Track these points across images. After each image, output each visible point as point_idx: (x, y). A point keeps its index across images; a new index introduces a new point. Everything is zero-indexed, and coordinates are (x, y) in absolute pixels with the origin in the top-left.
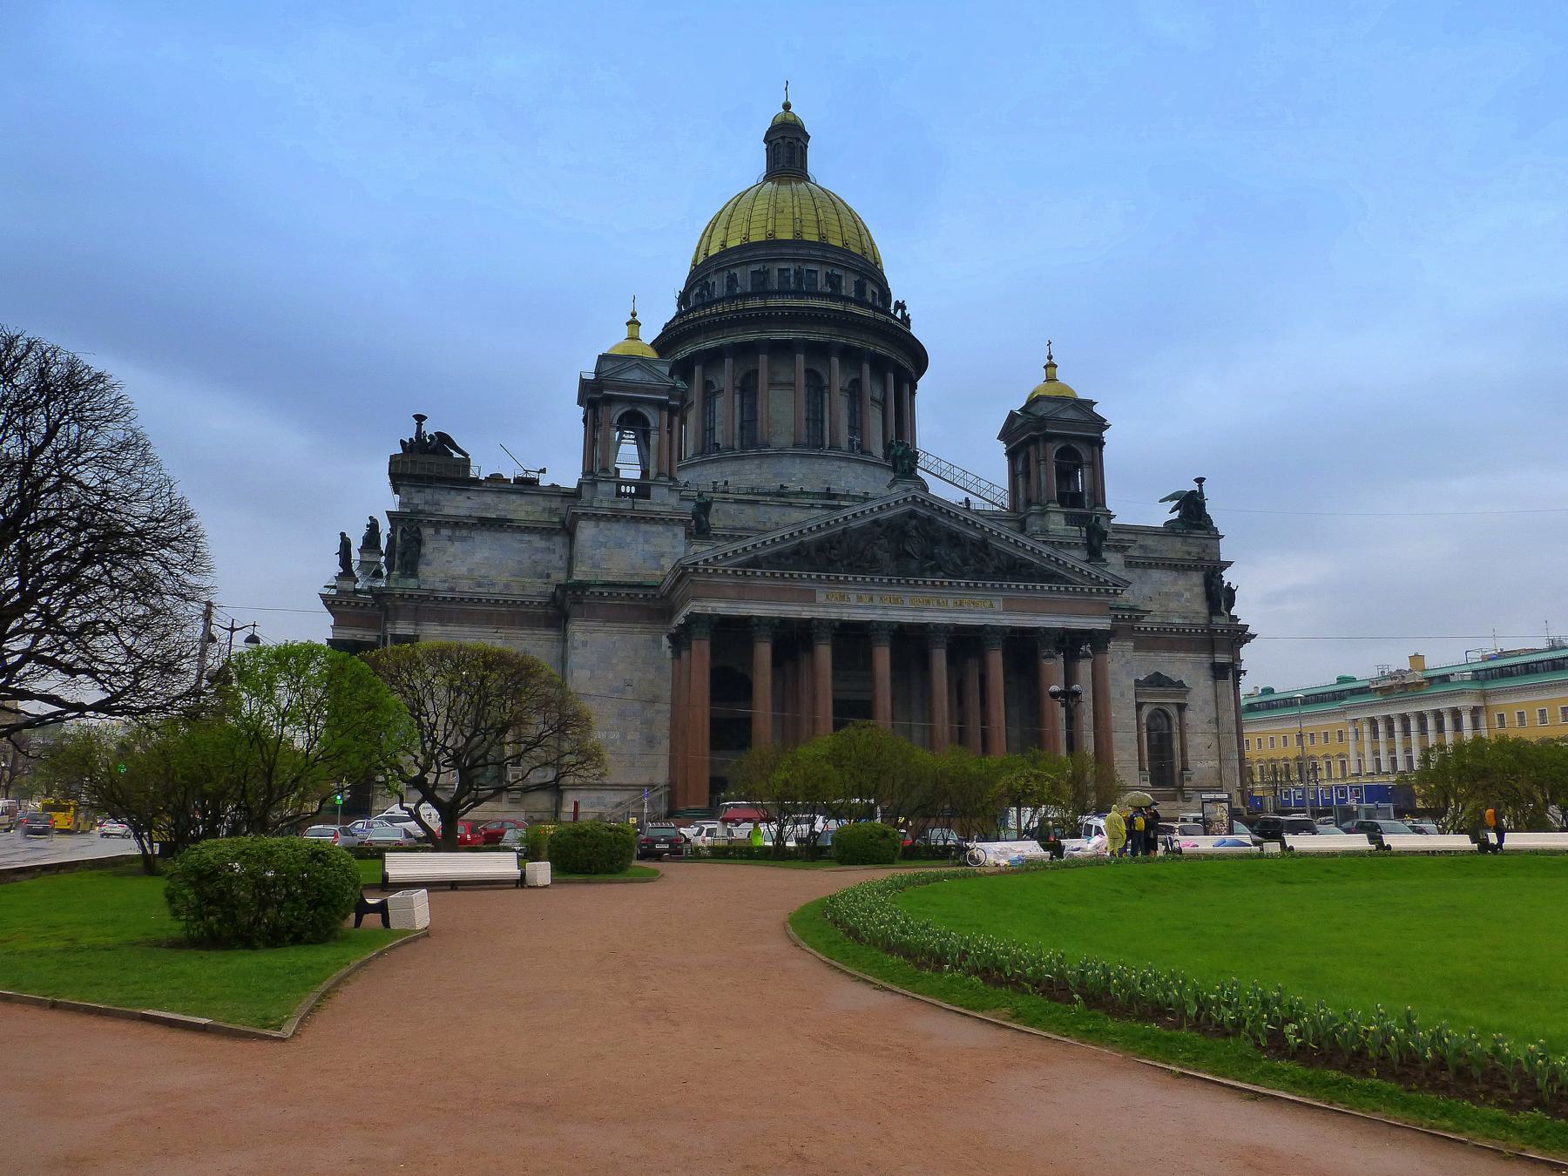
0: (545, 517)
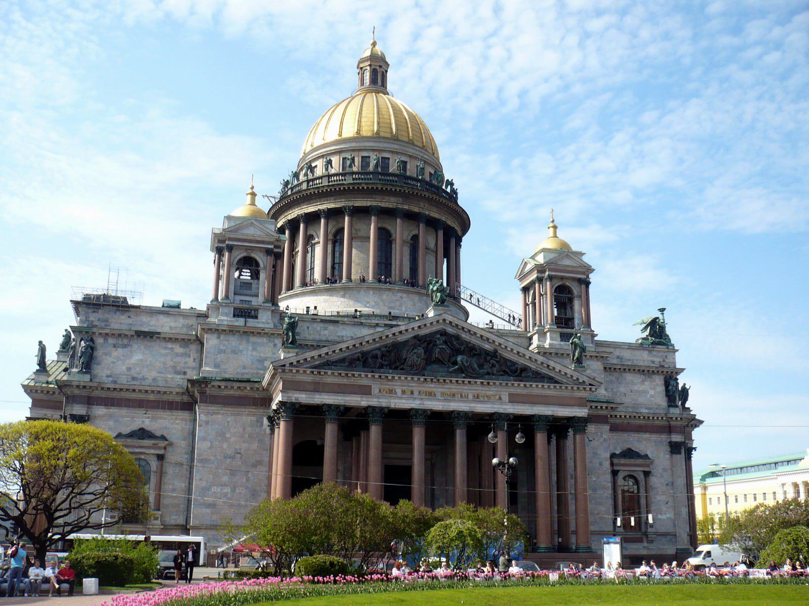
0: (184, 331)
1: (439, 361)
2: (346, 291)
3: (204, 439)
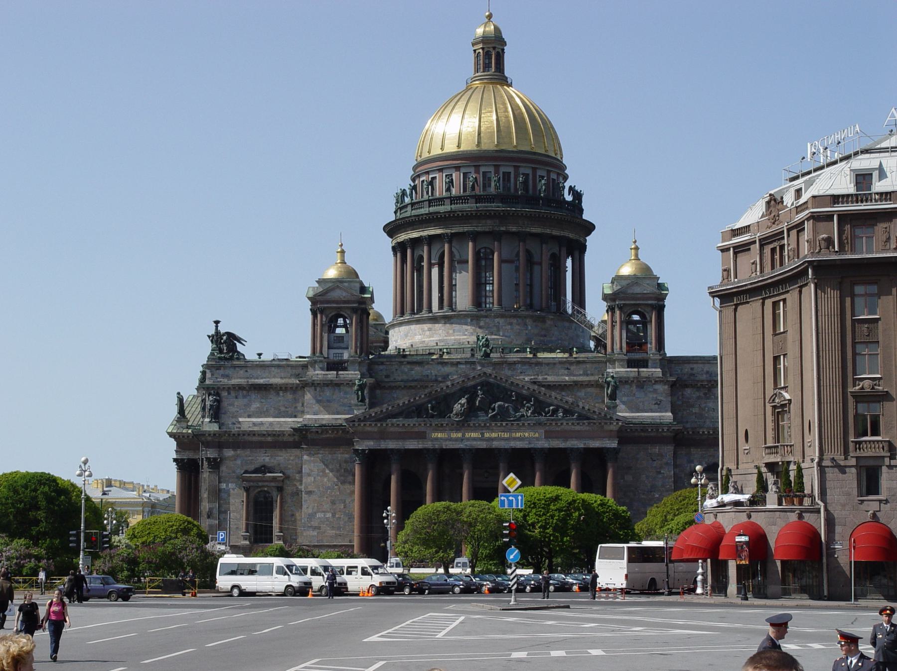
1: (480, 409)
2: (447, 319)
3: (309, 475)
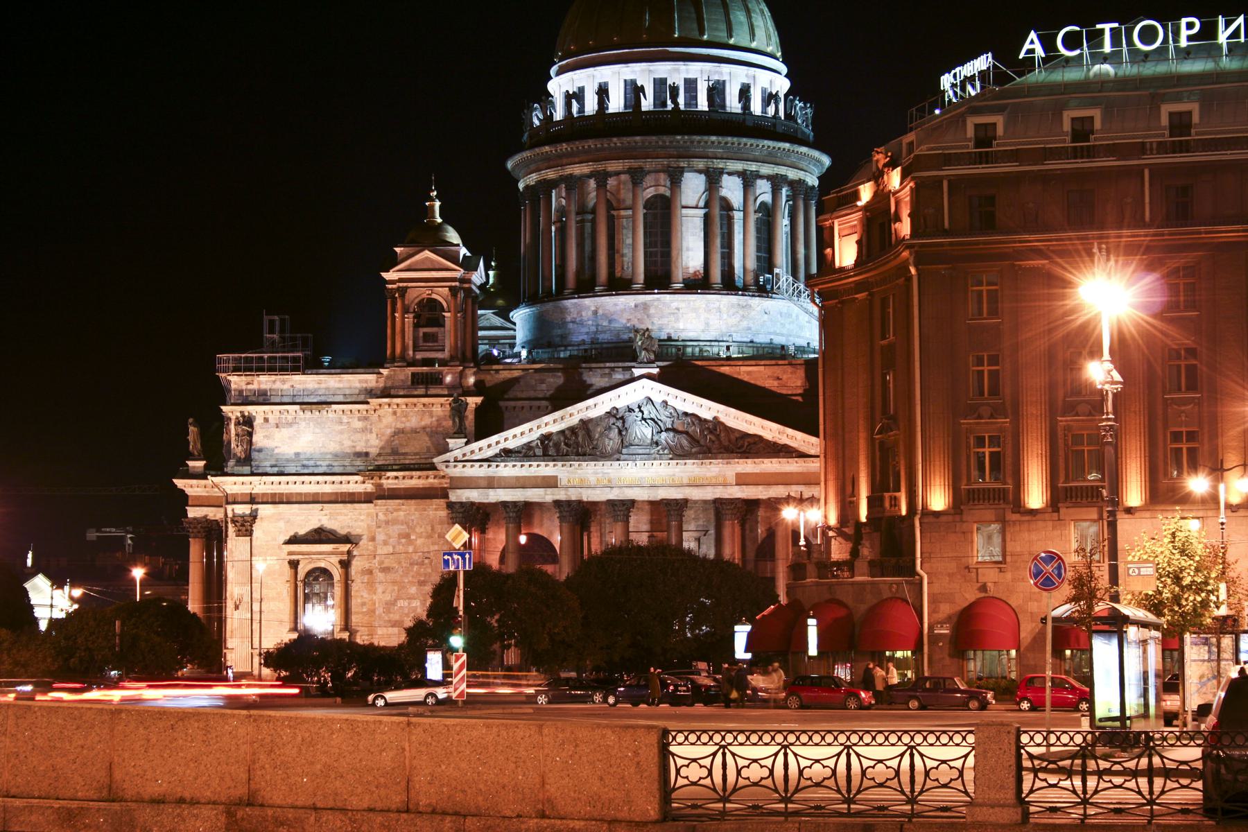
3: (385, 543)
